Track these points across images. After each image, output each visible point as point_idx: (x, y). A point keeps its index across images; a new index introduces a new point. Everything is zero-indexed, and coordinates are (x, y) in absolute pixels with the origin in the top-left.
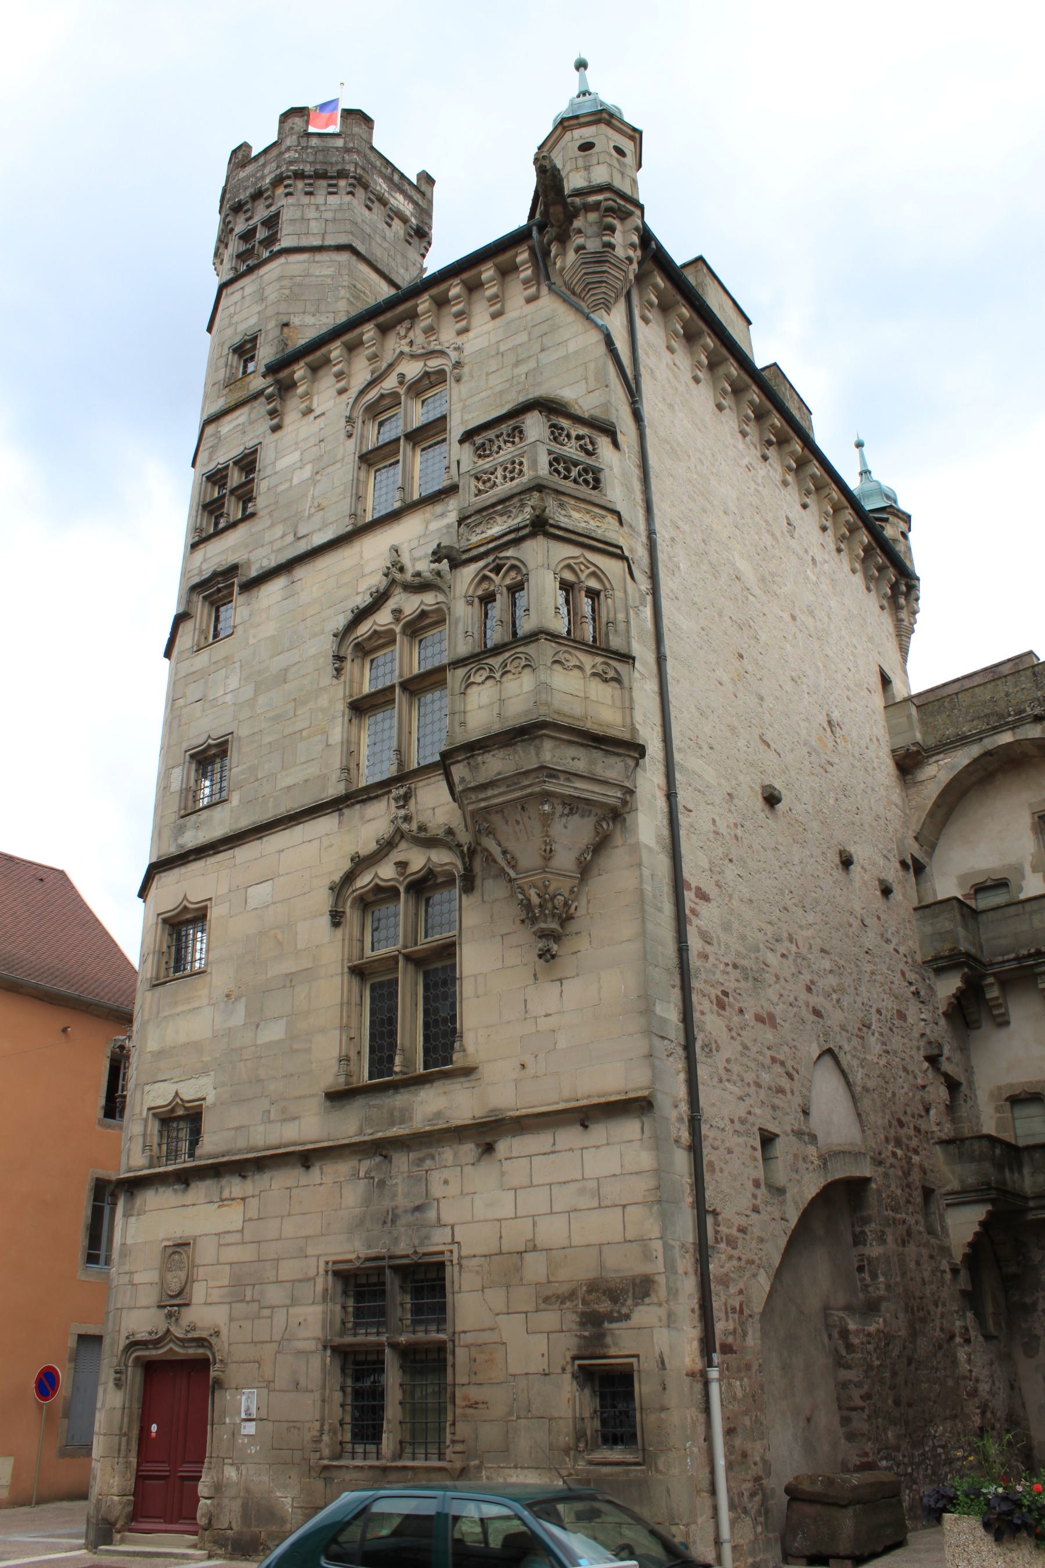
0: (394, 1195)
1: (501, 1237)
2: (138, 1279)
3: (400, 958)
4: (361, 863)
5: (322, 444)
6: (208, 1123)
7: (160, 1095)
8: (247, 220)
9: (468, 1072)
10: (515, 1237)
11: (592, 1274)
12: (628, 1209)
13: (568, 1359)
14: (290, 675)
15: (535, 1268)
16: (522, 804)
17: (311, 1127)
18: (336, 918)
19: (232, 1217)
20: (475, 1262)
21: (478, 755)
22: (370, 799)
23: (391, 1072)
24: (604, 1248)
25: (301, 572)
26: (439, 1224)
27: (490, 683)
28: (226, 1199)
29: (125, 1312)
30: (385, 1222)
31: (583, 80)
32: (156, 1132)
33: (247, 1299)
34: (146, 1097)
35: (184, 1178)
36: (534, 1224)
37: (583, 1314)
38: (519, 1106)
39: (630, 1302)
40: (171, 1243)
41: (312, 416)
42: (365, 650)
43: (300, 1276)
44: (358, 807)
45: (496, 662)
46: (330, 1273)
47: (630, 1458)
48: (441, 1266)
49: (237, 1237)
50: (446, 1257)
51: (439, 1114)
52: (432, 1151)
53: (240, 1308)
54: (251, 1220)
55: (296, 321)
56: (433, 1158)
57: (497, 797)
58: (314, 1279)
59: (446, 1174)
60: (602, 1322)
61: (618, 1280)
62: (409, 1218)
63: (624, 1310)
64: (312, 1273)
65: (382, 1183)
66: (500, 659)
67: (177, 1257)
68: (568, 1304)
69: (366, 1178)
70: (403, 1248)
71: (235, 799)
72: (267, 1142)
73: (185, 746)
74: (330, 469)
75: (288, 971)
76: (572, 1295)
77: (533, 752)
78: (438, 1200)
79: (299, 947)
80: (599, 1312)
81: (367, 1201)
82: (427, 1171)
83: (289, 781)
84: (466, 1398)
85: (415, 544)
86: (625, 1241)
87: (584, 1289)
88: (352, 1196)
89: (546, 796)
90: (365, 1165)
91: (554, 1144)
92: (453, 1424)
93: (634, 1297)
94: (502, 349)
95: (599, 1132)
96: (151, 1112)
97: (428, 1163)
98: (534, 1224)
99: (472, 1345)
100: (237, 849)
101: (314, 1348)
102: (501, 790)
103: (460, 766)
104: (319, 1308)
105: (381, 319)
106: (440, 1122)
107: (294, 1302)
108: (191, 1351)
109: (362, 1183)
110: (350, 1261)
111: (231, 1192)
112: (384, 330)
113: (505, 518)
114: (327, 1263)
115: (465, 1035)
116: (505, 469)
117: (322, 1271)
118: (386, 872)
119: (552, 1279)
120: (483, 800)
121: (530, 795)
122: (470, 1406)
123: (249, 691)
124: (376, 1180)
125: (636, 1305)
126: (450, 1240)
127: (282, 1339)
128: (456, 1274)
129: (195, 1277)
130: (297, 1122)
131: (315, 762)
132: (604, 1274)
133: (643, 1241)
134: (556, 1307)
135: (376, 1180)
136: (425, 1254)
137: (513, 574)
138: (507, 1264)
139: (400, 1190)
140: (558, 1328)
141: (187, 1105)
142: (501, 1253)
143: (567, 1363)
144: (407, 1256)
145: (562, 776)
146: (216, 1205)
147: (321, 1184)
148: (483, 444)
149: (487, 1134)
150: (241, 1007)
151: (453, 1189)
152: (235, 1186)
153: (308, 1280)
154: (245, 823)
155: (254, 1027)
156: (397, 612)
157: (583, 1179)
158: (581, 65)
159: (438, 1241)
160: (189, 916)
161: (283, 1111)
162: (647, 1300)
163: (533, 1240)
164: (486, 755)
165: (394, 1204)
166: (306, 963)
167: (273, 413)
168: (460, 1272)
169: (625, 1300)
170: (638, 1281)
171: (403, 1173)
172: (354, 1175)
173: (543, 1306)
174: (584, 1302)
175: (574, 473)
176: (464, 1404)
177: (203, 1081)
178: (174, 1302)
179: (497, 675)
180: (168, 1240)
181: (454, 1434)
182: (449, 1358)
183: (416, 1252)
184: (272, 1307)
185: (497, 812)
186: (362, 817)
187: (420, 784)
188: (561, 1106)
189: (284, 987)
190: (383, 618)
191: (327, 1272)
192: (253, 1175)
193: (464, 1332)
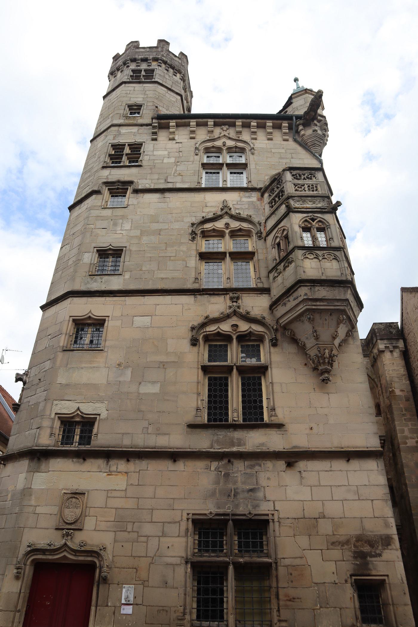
0: (235, 482)
1: (304, 510)
2: (39, 510)
3: (235, 367)
4: (209, 321)
5: (181, 153)
7: (67, 408)
8: (137, 66)
9: (279, 426)
10: (313, 510)
11: (358, 532)
12: (374, 502)
13: (349, 576)
14: (162, 233)
15: (325, 527)
16: (331, 312)
17: (177, 440)
18: (194, 342)
19: (119, 482)
21: (316, 286)
22: (214, 294)
23: (227, 420)
24: (364, 520)
25: (167, 195)
26: (265, 499)
27: (316, 260)
29: (26, 530)
30: (229, 496)
31: (297, 84)
32: (58, 427)
34: (54, 407)
35: (82, 456)
36: (323, 504)
37: (355, 552)
38: (310, 447)
39: (380, 548)
40: (69, 492)
41: (174, 142)
42: (205, 235)
43: (169, 520)
44: (206, 296)
45: (320, 253)
46: (190, 521)
48: (267, 522)
50: (271, 517)
51: (263, 444)
52: (260, 462)
53: (122, 535)
54: (131, 484)
55: (160, 108)
56: (260, 466)
57: (321, 306)
58: (179, 522)
59: (268, 474)
60: (367, 557)
62: (246, 495)
63: (378, 552)
64: (178, 519)
65: (227, 475)
66: (322, 252)
67: (74, 500)
68: (346, 547)
70: (241, 510)
71: (127, 276)
73: (94, 245)
74: (185, 163)
75: (162, 361)
76: (347, 542)
79: (169, 350)
80: (364, 552)
81: (217, 483)
82: (256, 472)
83: (163, 276)
84: (286, 595)
85: (235, 203)
86: (375, 517)
87: (354, 539)
89: (343, 312)
90: (214, 465)
91: (331, 467)
92: (278, 611)
93: (383, 545)
94: (273, 151)
95: (355, 464)
96: (57, 415)
98: (323, 504)
99: (289, 565)
100: (127, 298)
101: (179, 562)
102: (324, 304)
103: (306, 288)
105: (217, 120)
106: (264, 448)
107: (164, 535)
110: (205, 514)
111: (117, 468)
112: (216, 125)
113: (311, 203)
114: (188, 514)
116: (309, 186)
118: (225, 327)
119: (335, 533)
120: (315, 305)
121: (338, 309)
122: (290, 600)
123: (138, 233)
124: (223, 473)
125: (384, 549)
126: (273, 509)
127: (155, 555)
129: (87, 514)
130: (168, 436)
132: (364, 533)
133: (384, 518)
134: (339, 548)
135: (223, 473)
136: (256, 515)
137: (320, 224)
138: (309, 524)
139: (239, 479)
140: (341, 559)
141: (85, 416)
142: (304, 518)
143: (348, 578)
144: (245, 515)
145: (349, 307)
146: (106, 474)
148: (296, 175)
149: (292, 458)
153: (175, 522)
154: (132, 287)
155: (138, 384)
156: (227, 225)
157: (349, 485)
158: (296, 80)
159: (265, 508)
160: (89, 322)
162: (389, 547)
163: (323, 513)
164: (320, 287)
165: (235, 486)
166: (172, 359)
167: (154, 133)
168: (279, 526)
169: (378, 547)
170: (383, 537)
171: (241, 471)
172: (207, 469)
174: (355, 546)
176: (285, 599)
177: (98, 405)
178: (69, 528)
179: (320, 258)
180: (67, 489)
181: (279, 616)
182: (274, 572)
183: (250, 513)
184: (148, 537)
185: (318, 313)
186: (209, 301)
187: (244, 295)
188: (333, 449)
189: (159, 367)
190: (220, 225)
191: (188, 519)
193: (284, 558)
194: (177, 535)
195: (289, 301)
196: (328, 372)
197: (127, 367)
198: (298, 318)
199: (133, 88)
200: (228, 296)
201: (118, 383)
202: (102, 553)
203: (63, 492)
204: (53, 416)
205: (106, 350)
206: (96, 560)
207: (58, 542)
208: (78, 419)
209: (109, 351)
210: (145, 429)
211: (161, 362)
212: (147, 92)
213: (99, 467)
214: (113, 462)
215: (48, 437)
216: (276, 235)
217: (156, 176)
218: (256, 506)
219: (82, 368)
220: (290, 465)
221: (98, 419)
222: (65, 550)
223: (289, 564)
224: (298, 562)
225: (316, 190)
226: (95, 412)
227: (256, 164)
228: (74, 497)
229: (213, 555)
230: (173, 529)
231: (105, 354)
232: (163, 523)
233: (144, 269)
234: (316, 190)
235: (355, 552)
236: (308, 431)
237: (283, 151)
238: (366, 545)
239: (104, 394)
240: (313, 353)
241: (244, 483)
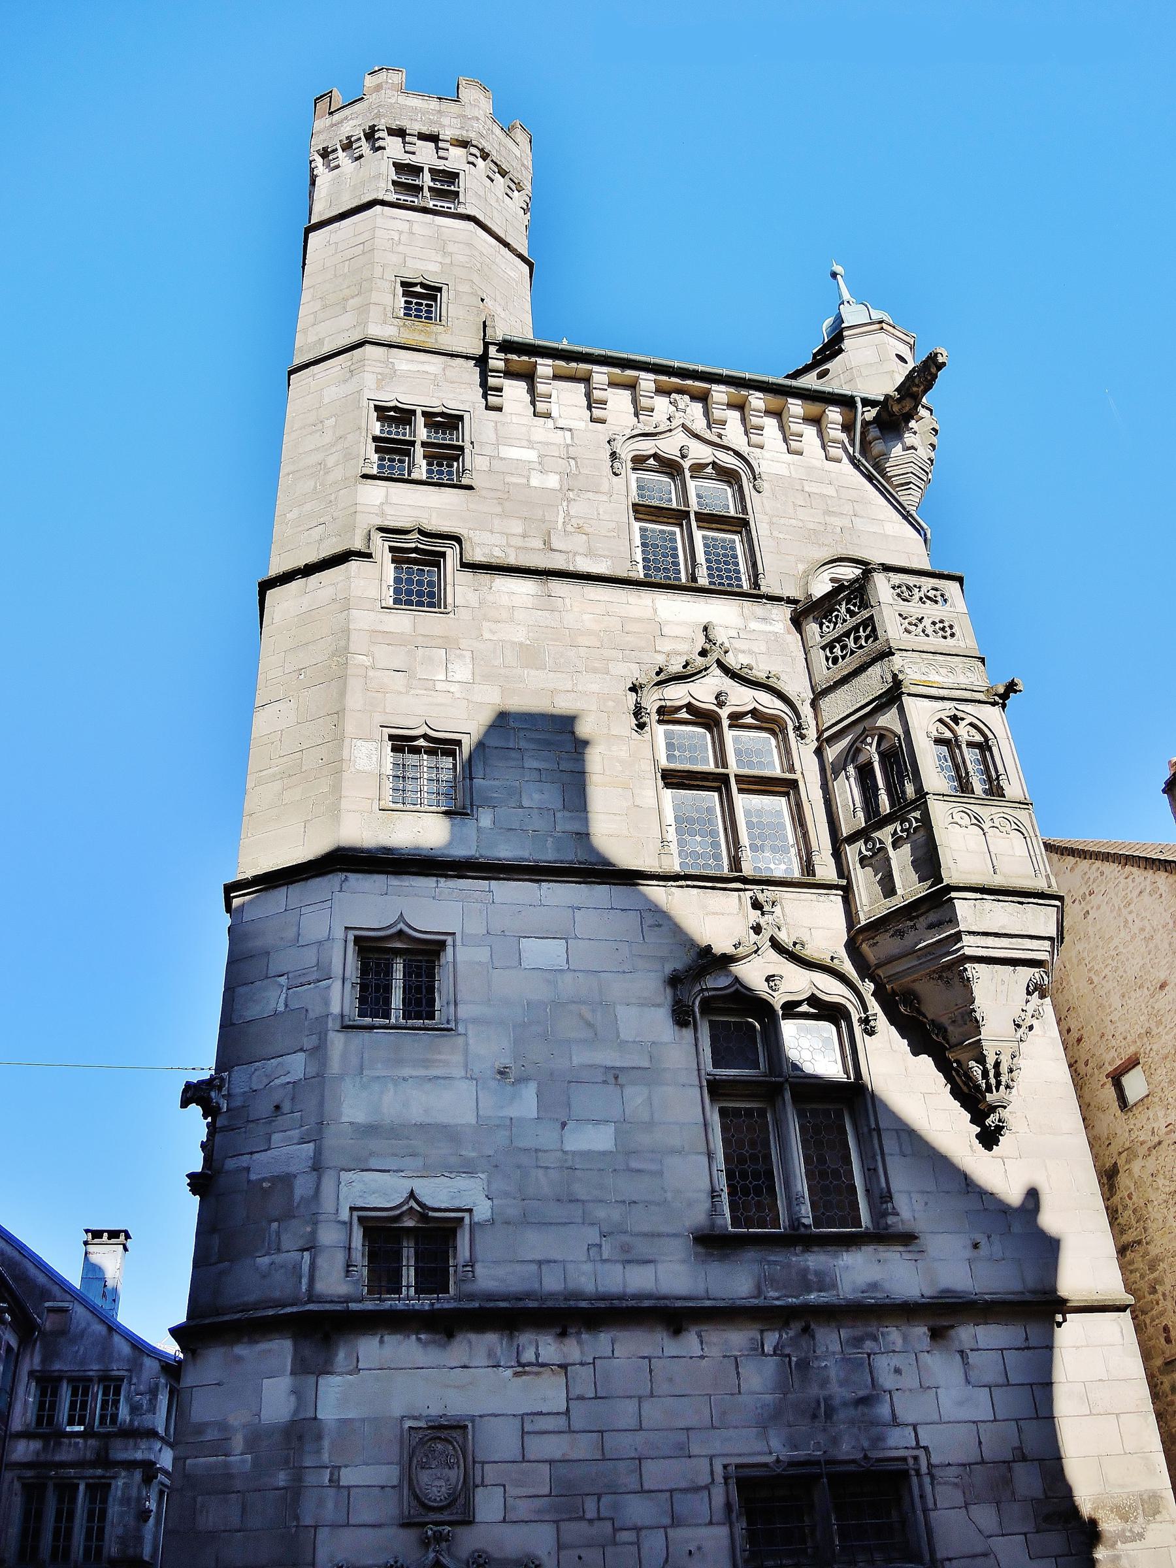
0: (824, 1383)
1: (980, 1443)
2: (348, 1477)
7: (382, 1190)
17: (675, 1275)
19: (549, 1393)
20: (952, 1471)
25: (558, 587)
26: (895, 1422)
29: (323, 1534)
33: (590, 1514)
34: (344, 1189)
35: (444, 1325)
39: (1141, 1519)
40: (422, 1424)
43: (683, 1485)
46: (732, 1481)
48: (904, 1475)
49: (561, 1422)
51: (874, 1286)
52: (872, 1329)
53: (574, 1530)
56: (875, 1339)
58: (707, 1488)
59: (896, 1361)
60: (1115, 1543)
61: (1125, 1496)
62: (852, 1412)
63: (1137, 1529)
64: (705, 1479)
65: (804, 1365)
69: (775, 1354)
70: (846, 1449)
71: (485, 819)
72: (601, 1289)
73: (380, 719)
75: (609, 1064)
77: (1042, 920)
78: (890, 1392)
82: (869, 1355)
88: (759, 1378)
90: (771, 1339)
91: (1027, 1339)
93: (1145, 1515)
94: (807, 489)
96: (355, 1214)
97: (869, 1345)
104: (723, 1531)
107: (676, 1521)
109: (771, 1364)
110: (765, 1465)
111: (537, 1355)
115: (895, 1196)
117: (719, 1479)
119: (1050, 1494)
126: (914, 1444)
128: (928, 1488)
129: (478, 1480)
130: (651, 1267)
131: (618, 818)
134: (1059, 1527)
141: (431, 1214)
144: (853, 1461)
146: (509, 1372)
147: (702, 1357)
151: (909, 1380)
153: (697, 1489)
155: (559, 1126)
160: (399, 945)
161: (625, 1249)
163: (1021, 1448)
165: (826, 1393)
168: (932, 1484)
170: (1145, 1497)
171: (834, 1353)
172: (756, 1349)
175: (851, 644)
180: (415, 1418)
183: (866, 1456)
184: (638, 1529)
189: (605, 1082)
191: (726, 1478)
192: (579, 1333)
193: (949, 1559)
194: (707, 1521)
195: (914, 927)
197: (522, 1080)
199: (405, 227)
200: (750, 894)
201: (508, 1122)
203: (408, 1424)
204: (345, 1215)
205: (461, 1029)
208: (410, 1223)
209: (470, 1033)
210: (593, 1251)
212: (451, 248)
214: (525, 1338)
215: (343, 1274)
217: (517, 527)
219: (404, 1079)
220: (937, 1334)
221: (467, 1221)
225: (953, 635)
226: (457, 1204)
227: (771, 523)
228: (439, 1438)
230: (698, 1505)
231: (460, 1040)
232: (671, 1491)
233: (526, 803)
234: (953, 635)
237: (830, 491)
238: (1112, 1516)
239: (474, 1154)
241: (842, 1384)
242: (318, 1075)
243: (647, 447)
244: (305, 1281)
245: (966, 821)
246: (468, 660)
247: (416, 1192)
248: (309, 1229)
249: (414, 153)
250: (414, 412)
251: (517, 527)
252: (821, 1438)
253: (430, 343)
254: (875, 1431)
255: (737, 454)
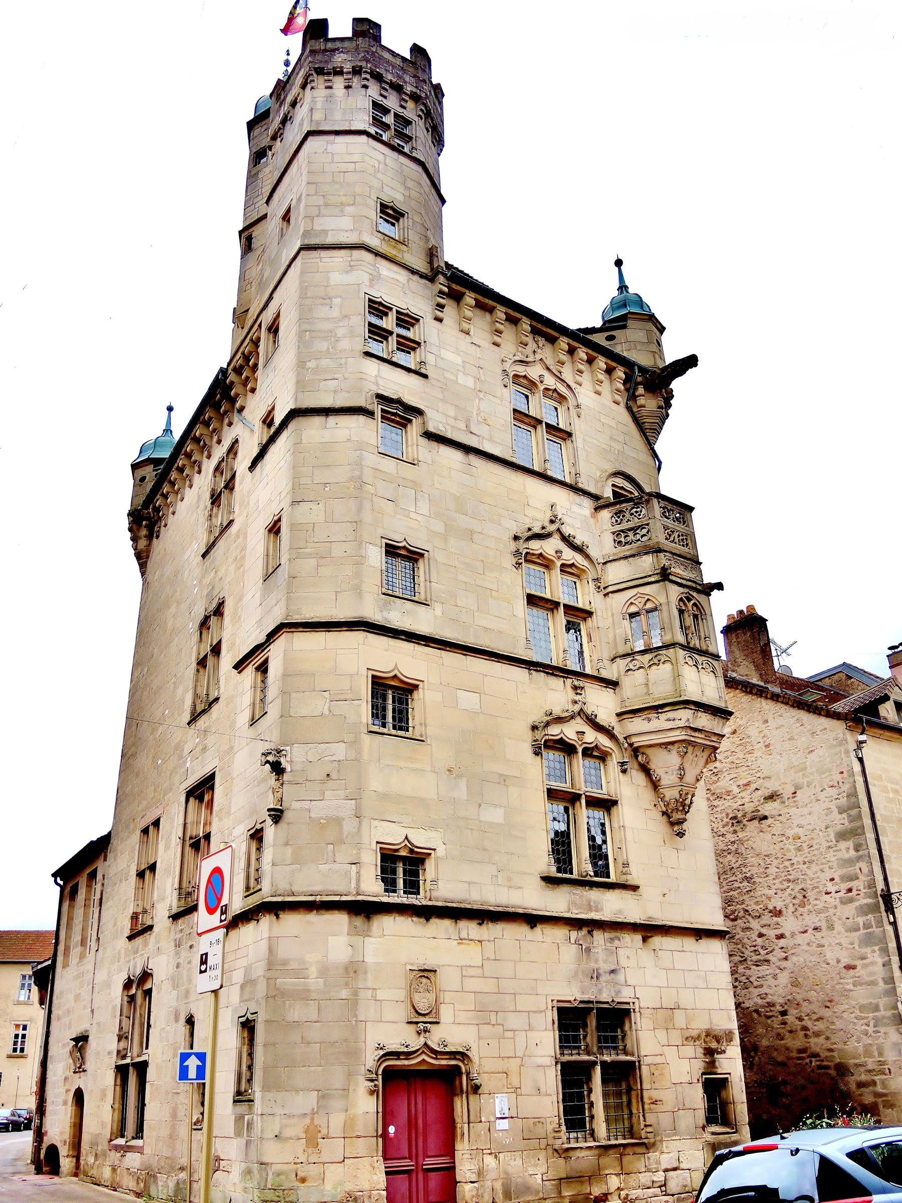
0: (596, 961)
2: (380, 995)
6: (429, 872)
15: (680, 1019)
19: (472, 955)
22: (552, 674)
25: (473, 459)
28: (465, 939)
34: (373, 831)
37: (705, 1049)
43: (534, 1009)
44: (542, 674)
46: (555, 1009)
47: (728, 1130)
49: (479, 972)
50: (632, 1006)
51: (620, 912)
54: (488, 959)
56: (619, 940)
58: (544, 1011)
59: (628, 952)
63: (723, 1048)
65: (588, 950)
67: (424, 980)
68: (697, 1043)
70: (605, 997)
71: (438, 609)
73: (380, 532)
75: (501, 773)
76: (699, 1037)
81: (579, 960)
83: (485, 623)
84: (650, 1098)
90: (574, 934)
96: (379, 845)
97: (616, 942)
101: (549, 1064)
107: (531, 1028)
108: (444, 1062)
110: (570, 1002)
111: (468, 934)
127: (524, 1055)
128: (638, 1018)
130: (520, 890)
136: (618, 1003)
141: (416, 850)
144: (607, 1003)
149: (648, 930)
150: (463, 784)
151: (632, 963)
152: (469, 928)
159: (626, 995)
173: (685, 1043)
174: (705, 1042)
177: (432, 834)
178: (423, 1019)
179: (700, 667)
180: (412, 964)
183: (613, 1001)
196: (680, 822)
197: (459, 776)
198: (666, 745)
199: (381, 158)
202: (468, 1053)
205: (429, 742)
206: (461, 1064)
207: (416, 1043)
210: (494, 879)
211: (501, 775)
213: (447, 930)
216: (632, 600)
218: (618, 992)
220: (645, 939)
221: (433, 855)
222: (423, 1052)
223: (650, 1062)
224: (659, 1060)
229: (574, 1052)
235: (705, 1049)
236: (661, 898)
240: (671, 794)
241: (605, 962)
242: (356, 760)
243: (521, 370)
244: (353, 882)
245: (691, 663)
246: (427, 501)
247: (409, 836)
248: (355, 852)
249: (385, 97)
250: (391, 309)
251: (452, 412)
252: (594, 989)
253: (399, 257)
254: (618, 987)
255: (569, 386)
